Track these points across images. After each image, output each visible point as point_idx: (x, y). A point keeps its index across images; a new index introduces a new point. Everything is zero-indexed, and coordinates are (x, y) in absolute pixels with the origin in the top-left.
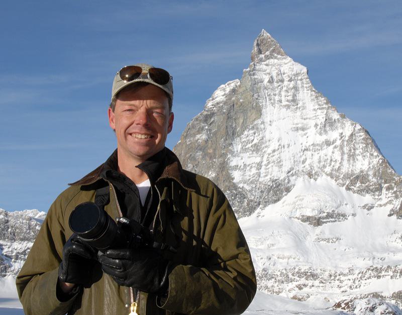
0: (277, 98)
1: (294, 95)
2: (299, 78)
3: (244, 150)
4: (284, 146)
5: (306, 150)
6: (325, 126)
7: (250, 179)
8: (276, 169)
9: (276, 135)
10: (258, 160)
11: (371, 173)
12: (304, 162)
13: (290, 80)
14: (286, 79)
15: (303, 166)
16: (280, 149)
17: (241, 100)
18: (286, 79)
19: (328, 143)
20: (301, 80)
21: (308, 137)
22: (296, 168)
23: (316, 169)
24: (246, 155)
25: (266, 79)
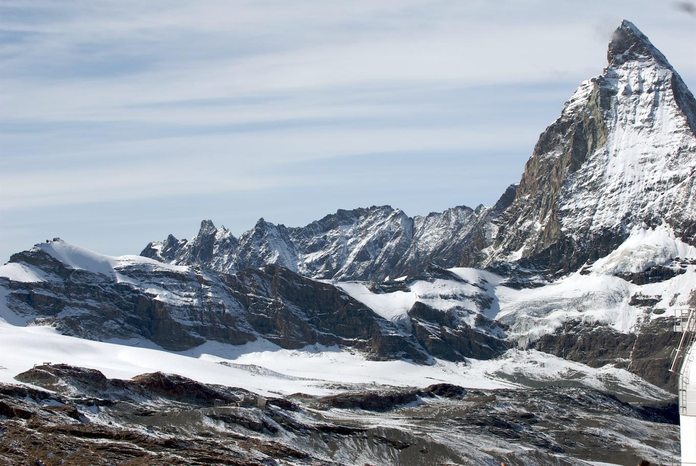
0: (630, 117)
1: (651, 114)
2: (661, 87)
3: (580, 189)
4: (625, 184)
5: (650, 189)
7: (579, 227)
8: (611, 213)
9: (619, 170)
10: (593, 202)
12: (644, 205)
13: (649, 91)
14: (646, 89)
15: (642, 210)
16: (620, 189)
17: (591, 117)
18: (646, 89)
19: (676, 180)
20: (664, 90)
21: (655, 172)
22: (634, 213)
23: (656, 214)
24: (580, 196)
25: (621, 87)
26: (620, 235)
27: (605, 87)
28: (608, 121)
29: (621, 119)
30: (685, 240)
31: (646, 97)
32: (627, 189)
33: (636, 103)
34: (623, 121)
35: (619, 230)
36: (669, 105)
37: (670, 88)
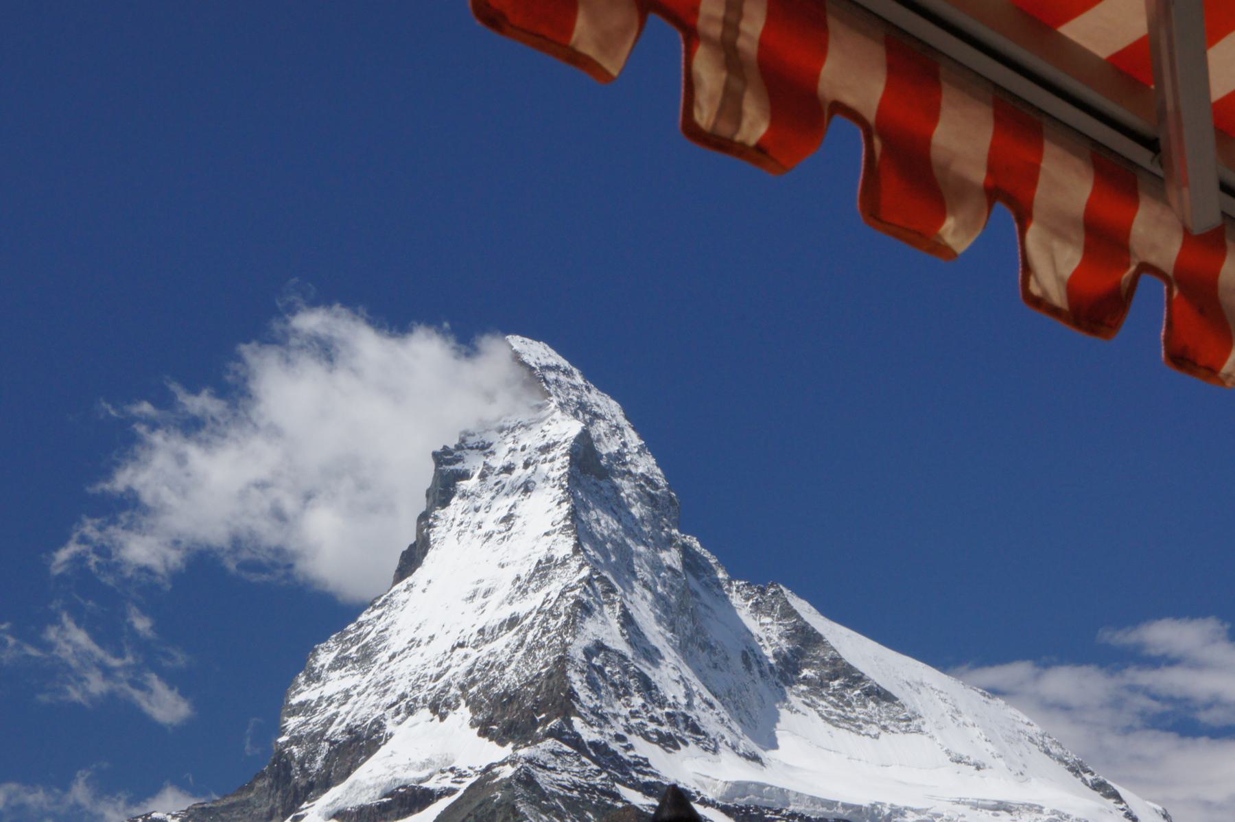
1: (514, 506)
2: (549, 456)
3: (339, 663)
5: (461, 645)
6: (529, 581)
12: (438, 677)
15: (431, 685)
20: (552, 460)
30: (484, 733)
32: (422, 648)
34: (462, 527)
37: (564, 455)
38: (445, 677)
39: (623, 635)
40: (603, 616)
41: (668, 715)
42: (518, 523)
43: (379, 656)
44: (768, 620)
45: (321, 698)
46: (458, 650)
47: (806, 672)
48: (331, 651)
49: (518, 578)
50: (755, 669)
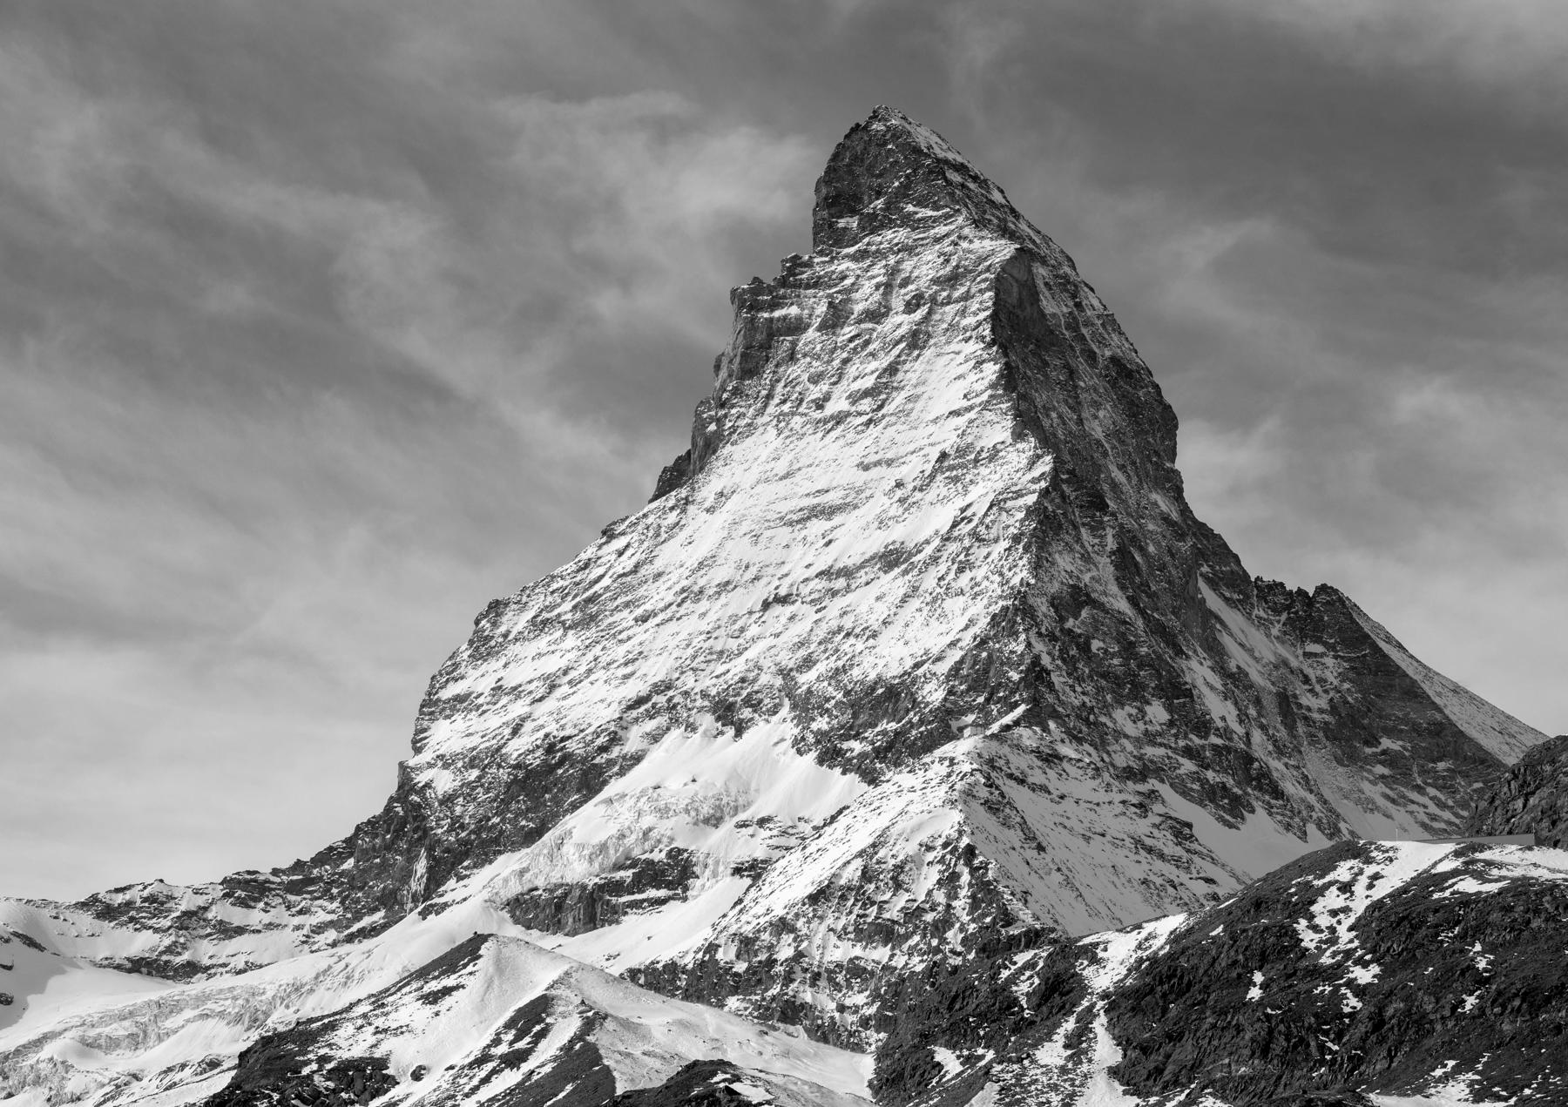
1: (892, 369)
2: (956, 294)
3: (540, 625)
5: (783, 600)
11: (943, 668)
13: (910, 307)
15: (720, 669)
16: (674, 607)
26: (597, 760)
27: (766, 315)
28: (733, 411)
29: (784, 402)
31: (900, 322)
32: (704, 605)
33: (855, 349)
34: (786, 408)
35: (599, 742)
36: (967, 340)
38: (750, 654)
39: (1123, 588)
40: (1083, 546)
41: (1215, 747)
42: (899, 399)
43: (617, 617)
44: (1317, 648)
45: (498, 690)
46: (777, 609)
47: (1386, 743)
48: (522, 610)
49: (899, 485)
50: (1301, 729)
